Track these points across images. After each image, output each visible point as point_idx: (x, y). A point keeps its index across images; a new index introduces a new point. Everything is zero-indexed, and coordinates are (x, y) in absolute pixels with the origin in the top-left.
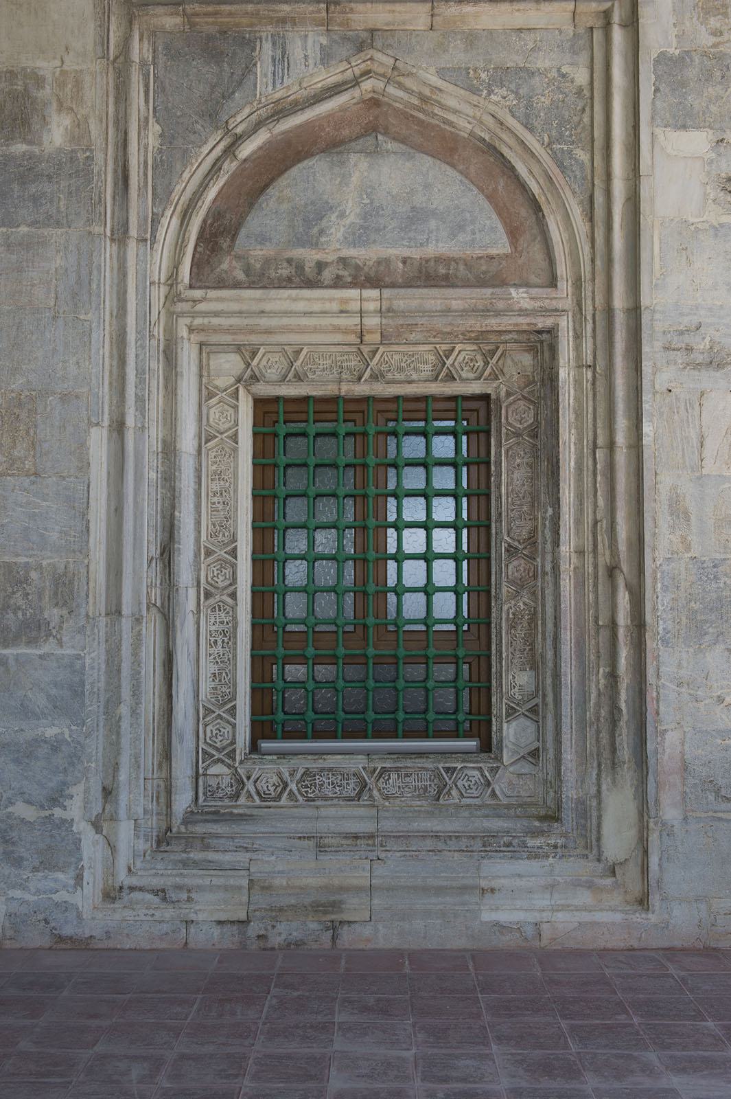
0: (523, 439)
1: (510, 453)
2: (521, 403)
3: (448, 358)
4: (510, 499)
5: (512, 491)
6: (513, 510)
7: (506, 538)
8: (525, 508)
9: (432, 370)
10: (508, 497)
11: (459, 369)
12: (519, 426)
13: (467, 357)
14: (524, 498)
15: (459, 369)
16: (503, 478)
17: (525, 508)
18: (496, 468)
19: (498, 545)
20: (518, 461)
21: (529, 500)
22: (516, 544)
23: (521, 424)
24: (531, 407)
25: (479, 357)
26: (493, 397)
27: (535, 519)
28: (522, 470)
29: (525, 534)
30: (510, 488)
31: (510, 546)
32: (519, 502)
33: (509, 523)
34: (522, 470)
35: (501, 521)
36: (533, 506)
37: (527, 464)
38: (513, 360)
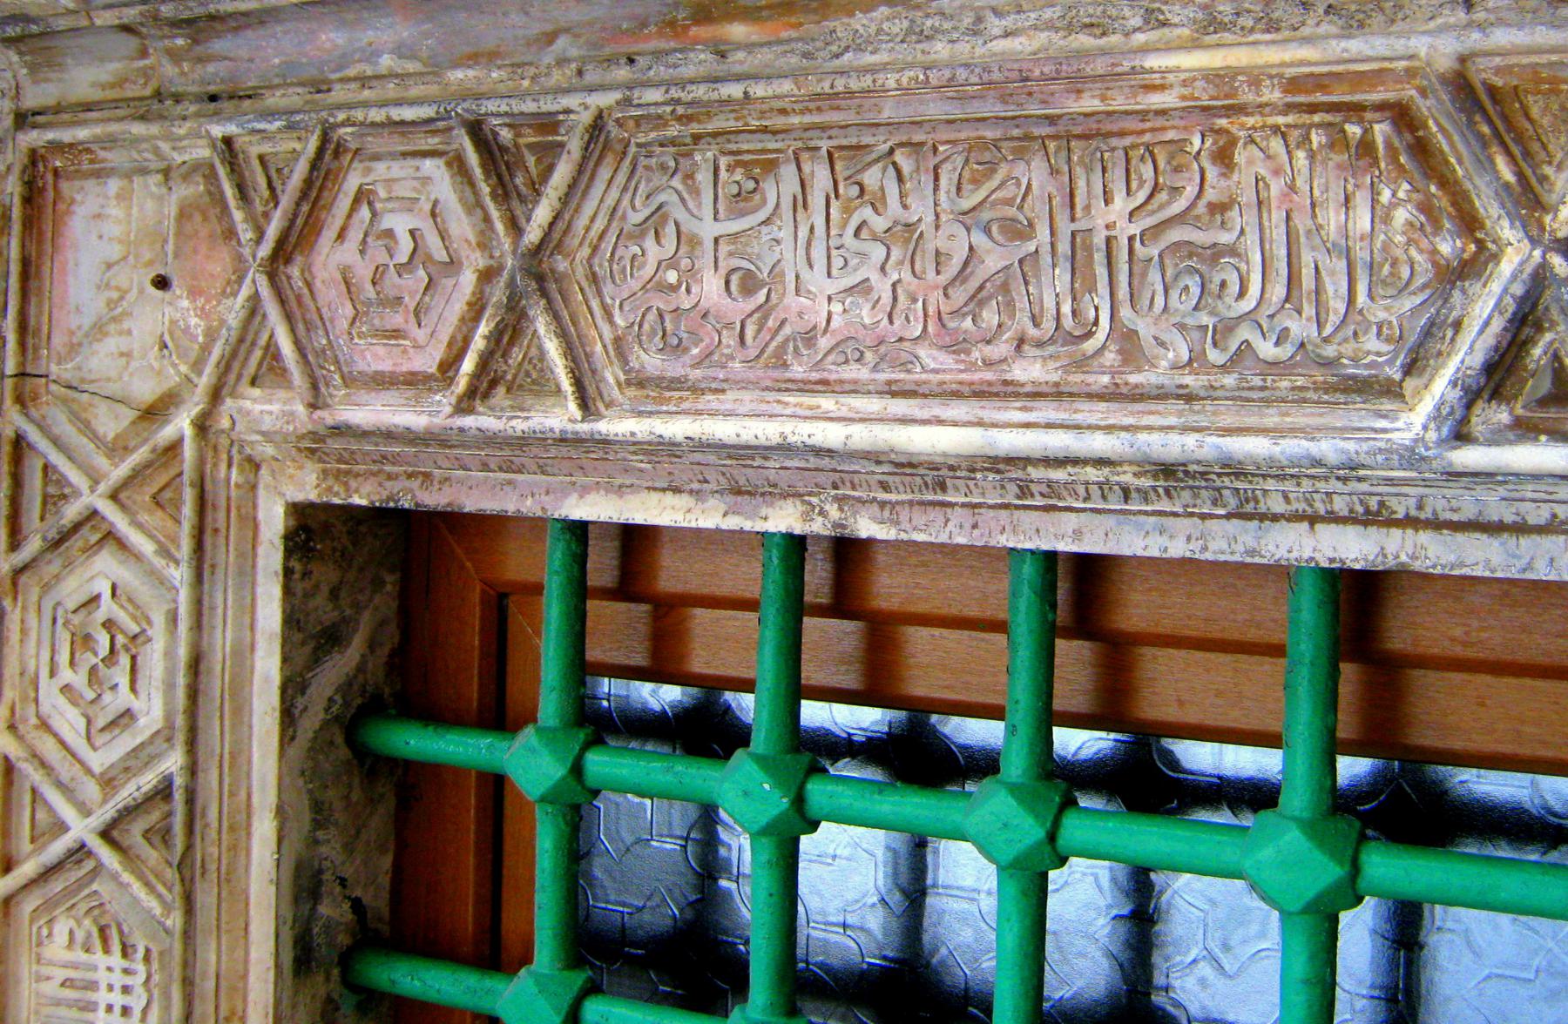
0: (553, 240)
1: (651, 361)
2: (331, 258)
3: (61, 827)
4: (1030, 371)
5: (957, 346)
6: (1127, 340)
7: (1414, 420)
8: (1114, 215)
9: (126, 952)
10: (1007, 392)
11: (126, 742)
12: (468, 280)
13: (66, 675)
14: (1018, 231)
15: (126, 742)
16: (830, 435)
17: (1114, 215)
18: (774, 493)
19: (1495, 506)
20: (710, 287)
21: (1035, 173)
22: (1483, 311)
23: (453, 265)
24: (353, 182)
25: (72, 590)
26: (307, 486)
27: (1220, 108)
28: (780, 248)
29: (1378, 215)
30: (934, 361)
31: (1498, 375)
32: (1055, 284)
33: (1260, 386)
34: (780, 248)
35: (1234, 469)
36: (1094, 132)
37: (742, 200)
38: (99, 330)
